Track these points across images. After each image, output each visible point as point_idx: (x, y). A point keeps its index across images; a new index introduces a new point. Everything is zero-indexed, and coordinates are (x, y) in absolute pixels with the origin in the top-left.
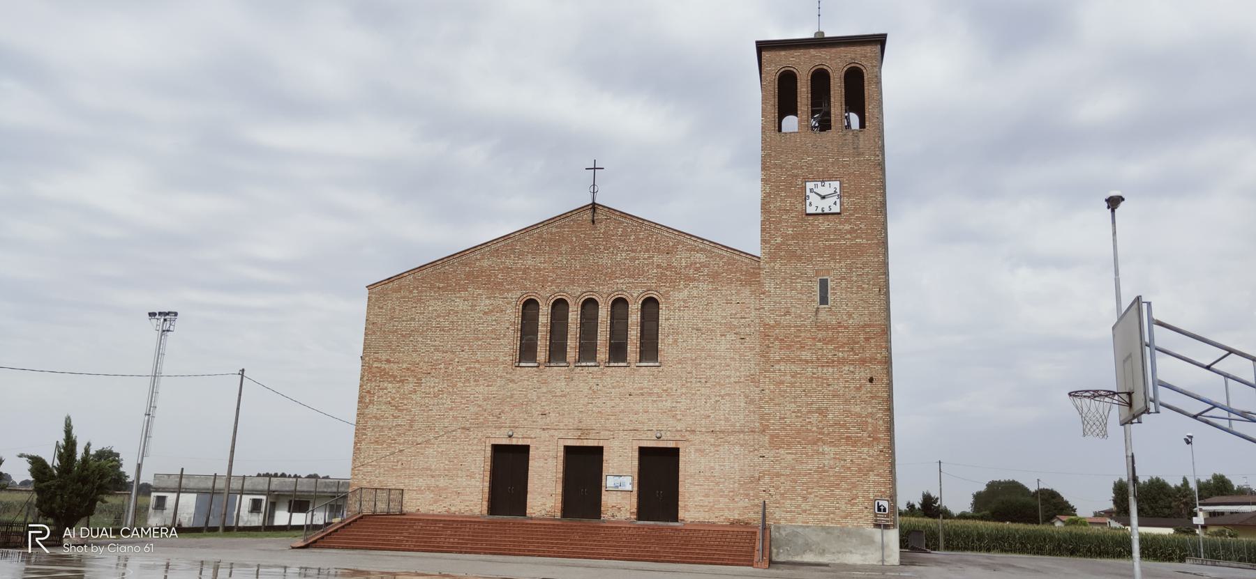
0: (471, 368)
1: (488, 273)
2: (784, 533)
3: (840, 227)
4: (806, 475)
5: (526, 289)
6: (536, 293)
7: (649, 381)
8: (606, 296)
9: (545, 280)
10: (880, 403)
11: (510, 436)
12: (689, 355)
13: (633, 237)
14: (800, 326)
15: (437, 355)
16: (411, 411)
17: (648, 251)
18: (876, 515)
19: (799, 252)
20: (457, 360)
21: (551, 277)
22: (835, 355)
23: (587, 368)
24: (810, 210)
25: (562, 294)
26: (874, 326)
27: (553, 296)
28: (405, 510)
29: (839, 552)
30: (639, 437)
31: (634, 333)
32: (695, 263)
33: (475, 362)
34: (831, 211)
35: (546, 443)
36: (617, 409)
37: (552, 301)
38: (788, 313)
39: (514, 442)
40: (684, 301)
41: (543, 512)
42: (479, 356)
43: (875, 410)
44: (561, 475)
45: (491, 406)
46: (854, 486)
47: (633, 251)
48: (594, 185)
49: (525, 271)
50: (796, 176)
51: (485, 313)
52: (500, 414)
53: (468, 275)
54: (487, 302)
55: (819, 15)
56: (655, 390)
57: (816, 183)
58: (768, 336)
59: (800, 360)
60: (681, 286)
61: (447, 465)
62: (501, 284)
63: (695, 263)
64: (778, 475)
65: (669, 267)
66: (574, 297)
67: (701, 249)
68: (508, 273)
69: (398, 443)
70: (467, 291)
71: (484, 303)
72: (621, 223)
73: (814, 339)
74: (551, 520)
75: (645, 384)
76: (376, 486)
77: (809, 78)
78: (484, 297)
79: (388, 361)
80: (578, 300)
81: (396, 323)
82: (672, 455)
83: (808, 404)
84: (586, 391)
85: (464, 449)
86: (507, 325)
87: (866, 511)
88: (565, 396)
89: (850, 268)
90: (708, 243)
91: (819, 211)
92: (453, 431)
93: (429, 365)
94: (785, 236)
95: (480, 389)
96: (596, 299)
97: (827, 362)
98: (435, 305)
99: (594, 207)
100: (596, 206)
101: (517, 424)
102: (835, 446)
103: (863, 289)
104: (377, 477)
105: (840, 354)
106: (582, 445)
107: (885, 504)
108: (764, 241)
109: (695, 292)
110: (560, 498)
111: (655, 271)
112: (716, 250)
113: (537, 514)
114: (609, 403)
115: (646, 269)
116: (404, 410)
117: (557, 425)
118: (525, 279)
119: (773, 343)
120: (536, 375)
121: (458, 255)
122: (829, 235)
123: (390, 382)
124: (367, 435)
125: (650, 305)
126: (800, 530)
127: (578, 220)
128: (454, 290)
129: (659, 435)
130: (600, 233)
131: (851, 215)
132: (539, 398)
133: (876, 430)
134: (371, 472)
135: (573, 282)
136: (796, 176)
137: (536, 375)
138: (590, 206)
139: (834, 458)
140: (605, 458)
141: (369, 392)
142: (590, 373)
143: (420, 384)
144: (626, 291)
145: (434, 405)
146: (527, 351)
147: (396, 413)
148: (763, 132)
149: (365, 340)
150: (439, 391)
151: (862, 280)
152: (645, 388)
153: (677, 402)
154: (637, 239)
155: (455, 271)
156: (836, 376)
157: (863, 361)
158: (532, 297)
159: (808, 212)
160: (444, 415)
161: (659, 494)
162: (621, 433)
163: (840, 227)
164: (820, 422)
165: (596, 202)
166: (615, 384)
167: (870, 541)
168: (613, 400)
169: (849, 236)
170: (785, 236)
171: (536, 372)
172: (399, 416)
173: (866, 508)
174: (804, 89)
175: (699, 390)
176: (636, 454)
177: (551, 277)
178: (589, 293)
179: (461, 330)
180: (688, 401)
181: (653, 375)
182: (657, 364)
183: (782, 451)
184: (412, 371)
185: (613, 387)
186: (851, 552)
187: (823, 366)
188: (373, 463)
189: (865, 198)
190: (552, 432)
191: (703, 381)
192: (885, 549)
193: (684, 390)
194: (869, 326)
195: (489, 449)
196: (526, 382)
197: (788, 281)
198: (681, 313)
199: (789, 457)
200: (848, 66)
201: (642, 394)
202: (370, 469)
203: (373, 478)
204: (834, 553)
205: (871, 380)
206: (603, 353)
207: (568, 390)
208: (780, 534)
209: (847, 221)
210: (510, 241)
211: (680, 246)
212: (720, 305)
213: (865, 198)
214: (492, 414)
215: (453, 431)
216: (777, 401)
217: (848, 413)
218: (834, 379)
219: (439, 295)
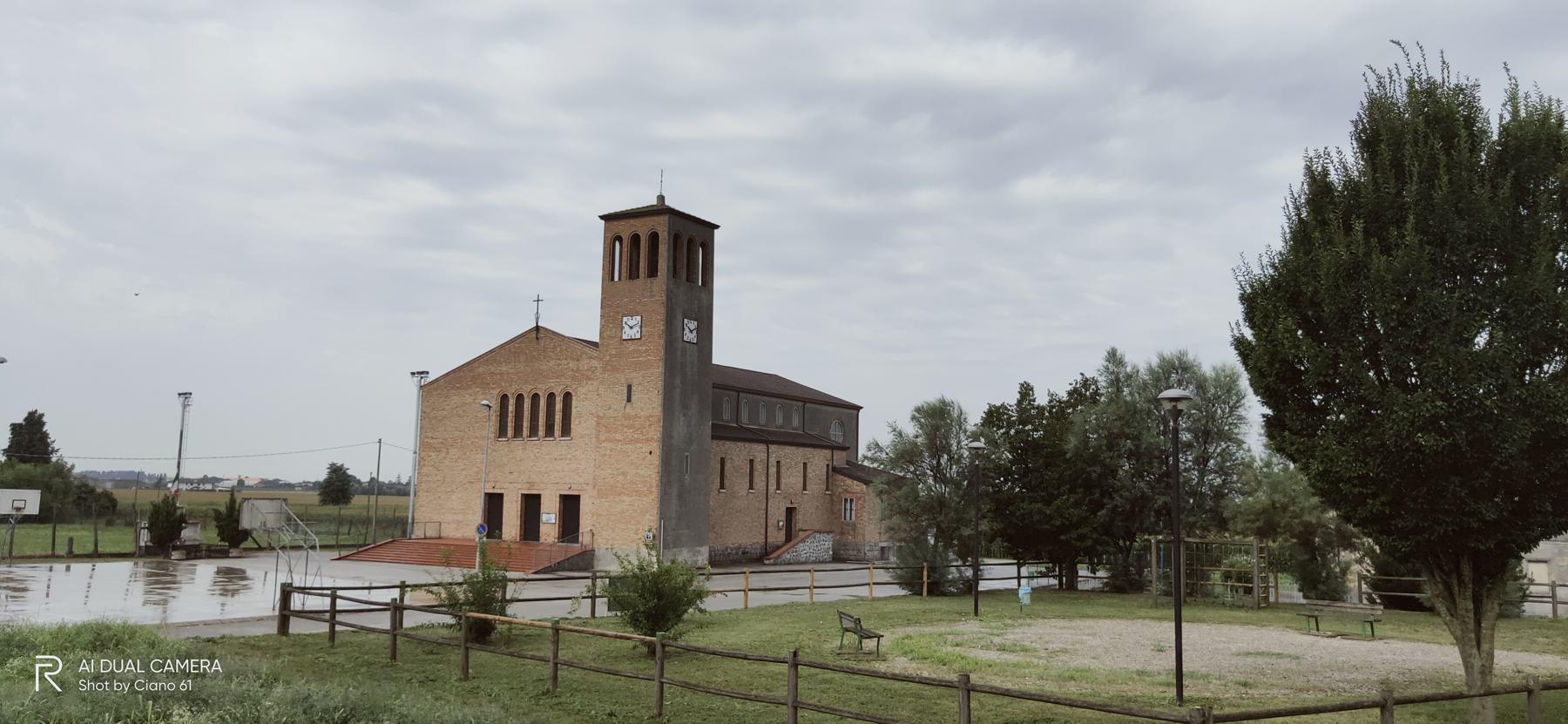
3: (640, 348)
15: (457, 433)
24: (625, 337)
28: (442, 535)
31: (558, 417)
36: (548, 469)
38: (610, 409)
39: (496, 491)
40: (586, 395)
42: (477, 434)
47: (559, 359)
49: (501, 374)
53: (473, 377)
56: (569, 456)
62: (488, 384)
65: (578, 370)
66: (527, 391)
72: (553, 339)
75: (564, 452)
79: (432, 438)
82: (577, 498)
95: (478, 456)
98: (455, 400)
99: (537, 328)
105: (635, 436)
110: (519, 528)
125: (567, 397)
133: (651, 486)
135: (526, 382)
143: (448, 453)
146: (502, 432)
147: (436, 472)
157: (647, 440)
163: (640, 348)
174: (626, 249)
176: (558, 499)
183: (603, 500)
185: (547, 454)
193: (584, 456)
194: (652, 416)
199: (607, 504)
201: (561, 459)
202: (424, 509)
216: (602, 467)
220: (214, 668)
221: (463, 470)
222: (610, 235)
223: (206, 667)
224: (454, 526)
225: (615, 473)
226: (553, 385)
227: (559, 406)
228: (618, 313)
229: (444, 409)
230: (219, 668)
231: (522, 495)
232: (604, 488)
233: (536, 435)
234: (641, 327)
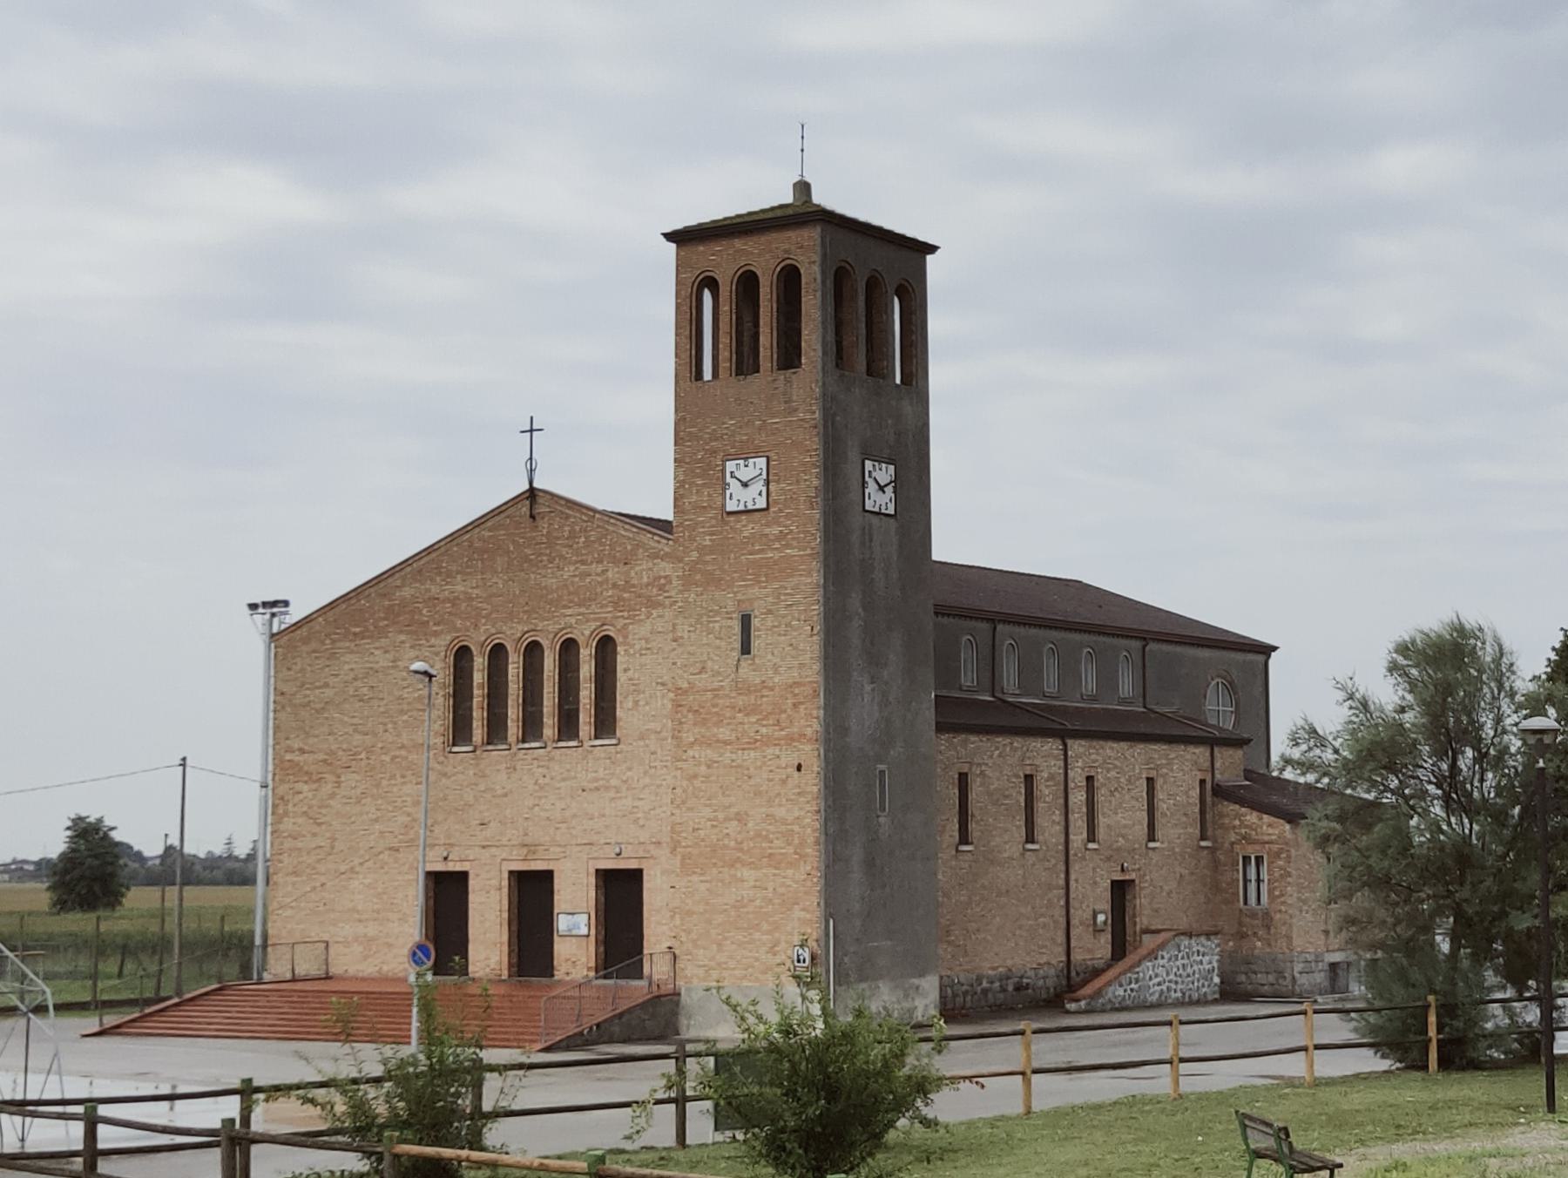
0: (396, 757)
3: (767, 531)
4: (721, 913)
5: (458, 630)
7: (605, 769)
8: (551, 636)
10: (808, 802)
13: (583, 539)
16: (331, 825)
17: (600, 561)
20: (380, 745)
24: (731, 506)
26: (804, 685)
28: (333, 971)
30: (596, 855)
31: (586, 694)
32: (660, 577)
35: (487, 868)
36: (568, 813)
38: (703, 670)
39: (452, 867)
40: (647, 640)
41: (488, 970)
42: (405, 739)
47: (583, 562)
48: (531, 459)
49: (454, 601)
56: (614, 782)
57: (738, 462)
59: (718, 741)
60: (643, 617)
65: (628, 585)
66: (513, 636)
68: (435, 606)
70: (387, 637)
72: (568, 517)
73: (733, 708)
75: (601, 773)
79: (302, 751)
81: (308, 692)
82: (635, 876)
84: (531, 787)
88: (505, 795)
91: (741, 507)
94: (701, 550)
97: (749, 743)
98: (350, 663)
99: (532, 494)
102: (755, 869)
105: (764, 730)
110: (505, 949)
111: (610, 593)
114: (560, 805)
115: (599, 590)
116: (322, 823)
118: (455, 615)
123: (306, 782)
125: (606, 647)
133: (802, 844)
138: (527, 495)
139: (755, 887)
140: (556, 887)
141: (282, 798)
143: (338, 784)
146: (460, 731)
147: (316, 829)
152: (603, 779)
154: (588, 544)
157: (790, 739)
159: (728, 509)
163: (767, 531)
164: (740, 833)
165: (536, 485)
170: (701, 550)
174: (727, 308)
175: (664, 780)
176: (593, 880)
178: (531, 634)
179: (383, 699)
182: (614, 741)
183: (695, 878)
184: (331, 764)
185: (564, 780)
187: (743, 749)
190: (493, 850)
193: (647, 780)
196: (460, 776)
199: (703, 887)
201: (597, 789)
202: (289, 912)
210: (434, 555)
218: (756, 768)
221: (376, 820)
222: (690, 276)
224: (357, 949)
225: (721, 816)
226: (573, 621)
227: (587, 669)
228: (714, 452)
229: (326, 685)
231: (511, 873)
232: (695, 851)
233: (538, 735)
234: (767, 482)
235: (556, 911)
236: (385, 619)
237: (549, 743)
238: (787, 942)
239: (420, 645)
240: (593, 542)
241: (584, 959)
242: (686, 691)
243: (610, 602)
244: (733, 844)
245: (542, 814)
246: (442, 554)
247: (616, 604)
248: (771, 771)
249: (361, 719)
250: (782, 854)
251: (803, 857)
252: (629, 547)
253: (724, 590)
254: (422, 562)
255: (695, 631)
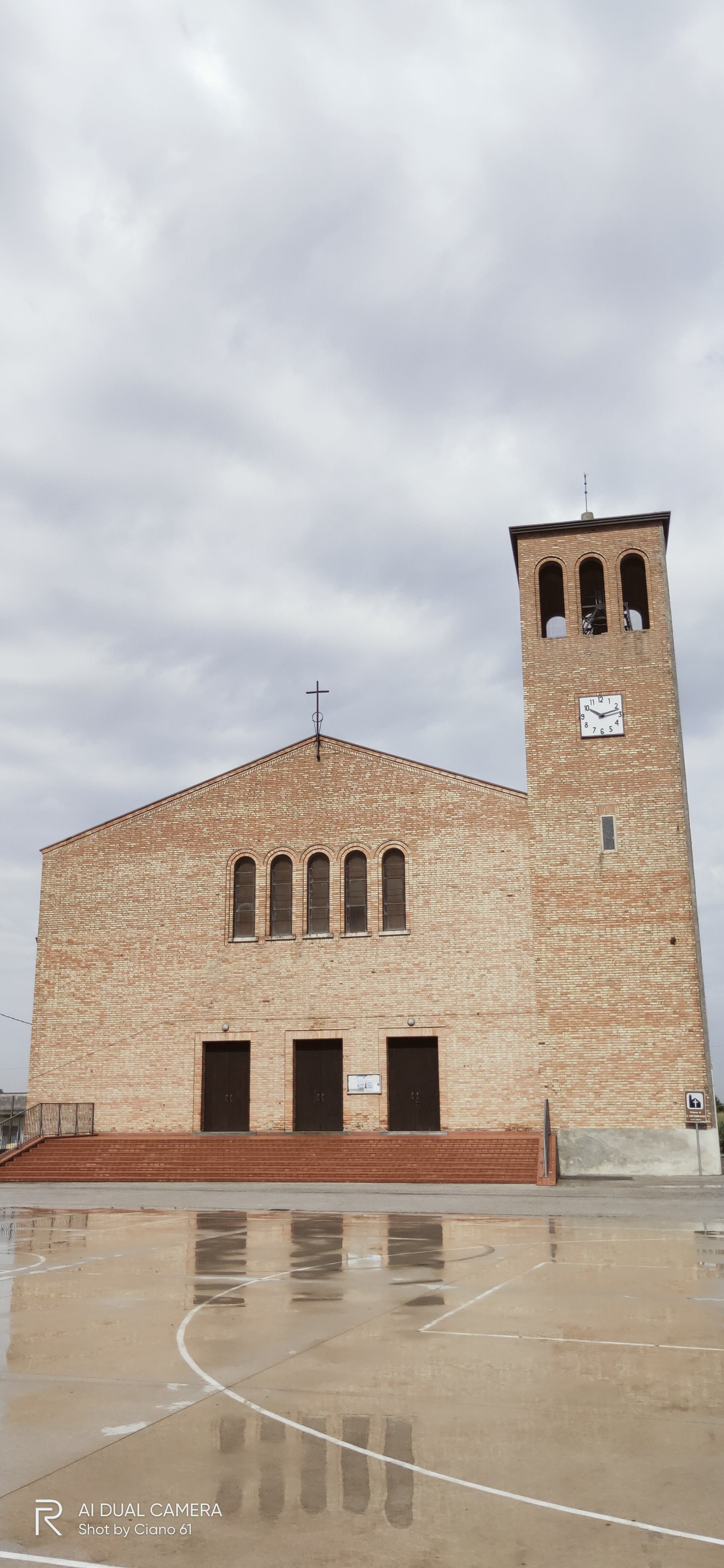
0: (173, 946)
1: (190, 826)
2: (573, 1139)
4: (597, 1065)
5: (238, 844)
6: (251, 850)
7: (396, 954)
8: (337, 849)
9: (261, 833)
10: (685, 970)
11: (225, 1031)
12: (444, 919)
13: (368, 775)
14: (580, 878)
15: (131, 933)
16: (101, 1004)
17: (388, 791)
18: (688, 1112)
19: (575, 785)
20: (155, 937)
21: (269, 828)
22: (626, 912)
23: (318, 940)
24: (586, 732)
25: (283, 849)
26: (672, 874)
27: (272, 853)
28: (97, 1129)
29: (644, 1161)
31: (375, 895)
32: (448, 804)
33: (178, 939)
34: (613, 733)
35: (271, 1037)
36: (358, 991)
37: (271, 859)
38: (564, 861)
39: (231, 1037)
40: (436, 852)
41: (271, 1125)
42: (182, 931)
43: (680, 979)
44: (290, 1077)
45: (200, 993)
46: (659, 1076)
47: (368, 792)
48: (318, 712)
49: (235, 822)
50: (567, 691)
51: (189, 877)
52: (212, 1003)
53: (169, 828)
54: (191, 863)
55: (586, 493)
56: (405, 965)
57: (592, 698)
58: (542, 891)
59: (583, 920)
60: (431, 834)
61: (148, 1070)
63: (448, 804)
64: (563, 1066)
65: (415, 810)
67: (454, 787)
68: (215, 826)
69: (86, 1045)
71: (187, 865)
72: (353, 757)
73: (599, 892)
74: (280, 1134)
75: (392, 958)
76: (60, 1100)
77: (577, 569)
78: (186, 857)
79: (70, 942)
80: (304, 856)
81: (78, 895)
83: (596, 975)
84: (318, 970)
85: (168, 1050)
86: (217, 891)
87: (675, 1107)
88: (291, 977)
89: (639, 801)
90: (461, 778)
91: (598, 733)
92: (154, 1027)
93: (121, 946)
94: (556, 766)
95: (187, 972)
96: (326, 853)
97: (617, 921)
98: (126, 870)
99: (318, 739)
100: (321, 738)
101: (233, 1015)
102: (632, 1026)
103: (657, 827)
104: (61, 1089)
105: (633, 911)
106: (315, 1037)
107: (699, 1097)
108: (531, 773)
109: (448, 840)
110: (290, 1106)
111: (398, 815)
112: (472, 787)
113: (262, 1128)
115: (386, 813)
116: (91, 1002)
117: (283, 1014)
118: (237, 832)
119: (547, 900)
120: (255, 952)
121: (153, 806)
122: (611, 762)
123: (73, 969)
124: (45, 1036)
126: (593, 1135)
127: (300, 757)
128: (149, 850)
129: (411, 1021)
130: (327, 771)
131: (638, 736)
132: (259, 981)
133: (682, 1004)
134: (53, 1083)
135: (296, 833)
136: (567, 691)
137: (255, 952)
138: (314, 739)
140: (345, 1053)
141: (47, 982)
142: (322, 947)
143: (110, 970)
144: (362, 843)
145: (129, 995)
147: (83, 1007)
148: (524, 639)
149: (41, 916)
150: (134, 977)
151: (655, 817)
153: (432, 979)
154: (374, 777)
155: (149, 826)
156: (629, 938)
157: (662, 918)
158: (247, 855)
159: (584, 735)
160: (141, 1007)
161: (415, 1096)
162: (364, 1021)
163: (624, 752)
164: (612, 996)
165: (321, 733)
166: (354, 959)
167: (682, 1146)
168: (352, 979)
169: (636, 763)
170: (556, 766)
171: (255, 948)
172: (86, 1011)
173: (676, 1103)
174: (572, 584)
175: (459, 963)
176: (384, 1047)
177: (269, 828)
178: (316, 847)
179: (160, 900)
180: (446, 978)
181: (401, 946)
182: (405, 932)
183: (566, 1035)
184: (100, 954)
185: (352, 963)
186: (659, 1160)
187: (612, 926)
188: (54, 1072)
189: (654, 715)
190: (278, 1023)
191: (464, 950)
192: (702, 1155)
193: (440, 964)
194: (667, 873)
195: (199, 1048)
196: (242, 962)
197: (563, 821)
198: (432, 867)
199: (576, 1043)
200: (625, 554)
202: (51, 1079)
203: (56, 1090)
204: (637, 1162)
205: (673, 941)
206: (337, 921)
207: (295, 970)
208: (569, 1141)
209: (633, 744)
210: (216, 786)
211: (428, 783)
212: (479, 855)
213: (654, 715)
214: (202, 1004)
215: (154, 1027)
216: (556, 972)
217: (646, 983)
219: (131, 857)
220: (214, 1512)
221: (150, 999)
223: (206, 1511)
224: (127, 1109)
225: (591, 982)
226: (360, 837)
230: (220, 1512)
232: (566, 1013)
233: (326, 928)
235: (345, 1074)
236: (163, 836)
237: (336, 934)
238: (671, 1089)
239: (200, 856)
240: (381, 776)
241: (376, 1114)
242: (548, 879)
243: (396, 822)
244: (605, 1005)
245: (329, 992)
246: (225, 786)
247: (404, 825)
248: (643, 944)
249: (135, 916)
250: (660, 1014)
251: (683, 1015)
252: (416, 781)
253: (583, 798)
254: (203, 791)
255: (553, 831)
